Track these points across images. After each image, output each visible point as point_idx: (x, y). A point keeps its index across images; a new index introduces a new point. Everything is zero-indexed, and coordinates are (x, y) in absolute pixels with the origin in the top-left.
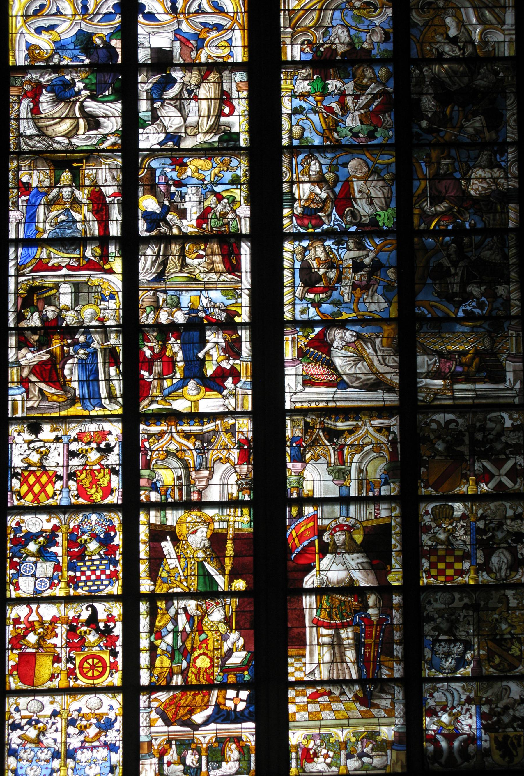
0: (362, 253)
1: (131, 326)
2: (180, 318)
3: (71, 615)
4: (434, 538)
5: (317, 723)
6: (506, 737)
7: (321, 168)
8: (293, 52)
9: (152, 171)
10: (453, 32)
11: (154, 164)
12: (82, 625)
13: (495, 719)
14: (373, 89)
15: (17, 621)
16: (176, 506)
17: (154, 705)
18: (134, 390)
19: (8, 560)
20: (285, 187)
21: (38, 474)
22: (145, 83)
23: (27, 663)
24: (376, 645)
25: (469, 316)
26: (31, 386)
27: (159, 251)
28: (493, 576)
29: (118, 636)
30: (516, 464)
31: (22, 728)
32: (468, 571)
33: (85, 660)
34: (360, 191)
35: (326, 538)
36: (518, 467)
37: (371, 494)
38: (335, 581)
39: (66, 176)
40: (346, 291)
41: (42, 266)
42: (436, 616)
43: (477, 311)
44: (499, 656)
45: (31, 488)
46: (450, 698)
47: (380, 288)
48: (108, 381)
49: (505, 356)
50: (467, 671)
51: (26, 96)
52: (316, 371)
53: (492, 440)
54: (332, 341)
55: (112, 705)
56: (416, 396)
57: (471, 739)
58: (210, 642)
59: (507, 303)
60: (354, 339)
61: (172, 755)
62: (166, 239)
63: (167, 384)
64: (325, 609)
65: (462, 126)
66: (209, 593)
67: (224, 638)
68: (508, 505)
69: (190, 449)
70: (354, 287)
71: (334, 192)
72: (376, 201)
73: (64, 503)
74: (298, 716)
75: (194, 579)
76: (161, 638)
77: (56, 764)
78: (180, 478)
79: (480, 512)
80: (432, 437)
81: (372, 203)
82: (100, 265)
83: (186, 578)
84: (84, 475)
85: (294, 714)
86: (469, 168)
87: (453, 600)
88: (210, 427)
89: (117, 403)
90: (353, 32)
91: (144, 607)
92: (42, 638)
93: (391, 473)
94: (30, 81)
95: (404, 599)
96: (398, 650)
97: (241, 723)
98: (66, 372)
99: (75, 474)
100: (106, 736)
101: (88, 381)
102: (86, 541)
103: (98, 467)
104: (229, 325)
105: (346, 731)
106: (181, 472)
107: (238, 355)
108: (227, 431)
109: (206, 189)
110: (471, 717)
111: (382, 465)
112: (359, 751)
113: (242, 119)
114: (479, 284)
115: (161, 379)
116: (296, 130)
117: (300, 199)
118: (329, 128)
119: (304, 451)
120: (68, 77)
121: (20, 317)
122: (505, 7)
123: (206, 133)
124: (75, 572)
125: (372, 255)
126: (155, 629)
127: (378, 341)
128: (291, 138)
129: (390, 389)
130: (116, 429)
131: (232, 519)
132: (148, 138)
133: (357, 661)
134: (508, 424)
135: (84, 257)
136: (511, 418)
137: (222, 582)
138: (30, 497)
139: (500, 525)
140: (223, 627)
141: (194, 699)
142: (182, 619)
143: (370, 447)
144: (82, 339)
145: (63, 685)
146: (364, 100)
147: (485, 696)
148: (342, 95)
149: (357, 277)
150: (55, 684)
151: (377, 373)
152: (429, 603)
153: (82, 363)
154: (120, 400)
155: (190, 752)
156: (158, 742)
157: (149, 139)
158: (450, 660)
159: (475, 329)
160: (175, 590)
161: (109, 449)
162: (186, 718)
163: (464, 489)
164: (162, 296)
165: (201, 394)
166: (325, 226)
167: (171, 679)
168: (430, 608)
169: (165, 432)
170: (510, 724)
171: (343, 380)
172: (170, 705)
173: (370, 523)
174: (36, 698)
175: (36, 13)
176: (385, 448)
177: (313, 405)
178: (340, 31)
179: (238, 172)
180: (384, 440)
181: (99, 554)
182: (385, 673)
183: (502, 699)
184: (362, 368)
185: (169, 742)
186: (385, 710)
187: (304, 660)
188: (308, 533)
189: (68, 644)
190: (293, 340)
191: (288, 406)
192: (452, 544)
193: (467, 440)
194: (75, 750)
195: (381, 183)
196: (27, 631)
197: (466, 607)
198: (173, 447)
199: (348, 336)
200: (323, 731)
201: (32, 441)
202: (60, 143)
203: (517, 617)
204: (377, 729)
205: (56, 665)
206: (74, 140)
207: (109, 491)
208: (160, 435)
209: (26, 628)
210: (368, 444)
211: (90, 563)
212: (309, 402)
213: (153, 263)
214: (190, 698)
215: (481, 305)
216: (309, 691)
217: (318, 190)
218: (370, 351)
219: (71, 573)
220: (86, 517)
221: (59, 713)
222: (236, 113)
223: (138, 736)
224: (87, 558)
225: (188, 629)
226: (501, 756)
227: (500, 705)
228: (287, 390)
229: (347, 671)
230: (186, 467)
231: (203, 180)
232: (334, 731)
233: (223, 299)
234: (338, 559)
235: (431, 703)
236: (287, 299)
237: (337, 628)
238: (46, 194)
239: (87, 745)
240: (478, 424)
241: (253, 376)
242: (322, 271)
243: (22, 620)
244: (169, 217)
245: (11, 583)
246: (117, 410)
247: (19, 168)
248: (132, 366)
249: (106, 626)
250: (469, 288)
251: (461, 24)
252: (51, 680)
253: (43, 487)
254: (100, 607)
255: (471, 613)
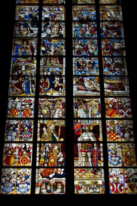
0: (91, 60)
1: (38, 76)
2: (49, 74)
3: (20, 146)
4: (110, 129)
5: (82, 179)
6: (131, 185)
7: (81, 42)
8: (75, 19)
9: (44, 42)
10: (109, 16)
11: (45, 40)
12: (23, 149)
13: (128, 179)
14: (92, 26)
15: (6, 147)
16: (47, 119)
17: (40, 172)
18: (38, 90)
19: (6, 131)
20: (73, 46)
21: (14, 110)
22: (43, 24)
23: (8, 159)
24: (96, 157)
25: (116, 75)
26: (14, 89)
27: (45, 59)
28: (125, 139)
29: (31, 152)
30: (129, 111)
31: (5, 177)
32: (119, 138)
33: (22, 159)
34: (90, 47)
35: (83, 128)
36: (130, 112)
37: (94, 117)
38: (86, 139)
39: (25, 42)
40: (87, 69)
41: (19, 61)
42: (111, 150)
43: (118, 74)
44: (128, 161)
45: (12, 113)
46: (116, 173)
47: (95, 68)
48: (32, 88)
49: (125, 85)
50: (120, 165)
51: (18, 26)
52: (80, 87)
53: (123, 105)
54: (84, 80)
55: (29, 172)
56: (104, 93)
57: (122, 185)
58: (54, 155)
59: (124, 72)
60: (89, 80)
61: (44, 186)
62: (47, 56)
63: (46, 89)
64: (83, 147)
65: (112, 34)
66: (54, 142)
67: (58, 154)
68: (128, 121)
69: (50, 105)
70: (89, 68)
71: (84, 47)
72: (93, 49)
73: (20, 117)
74: (77, 177)
75: (51, 138)
76: (42, 153)
77: (14, 188)
78: (48, 112)
79: (121, 123)
80: (108, 103)
81: (93, 50)
82: (32, 61)
83: (49, 137)
84: (25, 110)
85: (76, 176)
86: (114, 43)
87: (116, 145)
88: (55, 99)
89: (34, 93)
90: (87, 15)
91: (38, 145)
92: (12, 152)
93: (99, 112)
94: (19, 23)
95: (103, 145)
96: (102, 159)
97: (62, 178)
98: (22, 85)
99: (23, 110)
100: (27, 180)
101: (27, 88)
102: (25, 127)
103: (28, 108)
104: (60, 76)
105: (90, 181)
106: (48, 110)
107: (62, 83)
108: (59, 101)
109: (56, 46)
110: (122, 178)
111: (97, 110)
112: (93, 187)
113: (64, 32)
114: (118, 68)
115: (44, 88)
116: (75, 34)
117: (77, 48)
118: (83, 34)
119: (78, 106)
120: (27, 23)
121: (13, 73)
122: (120, 11)
123: (56, 34)
124: (22, 135)
125: (93, 61)
126: (41, 151)
127: (95, 80)
128: (74, 36)
129: (98, 92)
130: (33, 99)
131: (60, 122)
132: (43, 35)
133: (92, 161)
134: (127, 101)
135: (28, 60)
136: (127, 99)
137: (57, 138)
138: (12, 115)
139: (126, 126)
140: (58, 151)
141: (50, 170)
142: (47, 148)
143: (94, 105)
144: (26, 78)
145: (17, 165)
146: (90, 29)
147: (125, 172)
148: (86, 27)
149: (90, 66)
150: (15, 165)
151: (95, 88)
152: (110, 146)
153: (26, 84)
154: (35, 92)
155: (48, 186)
156: (40, 182)
157: (44, 35)
158: (115, 162)
159: (117, 78)
160: (46, 141)
161: (31, 104)
162: (47, 176)
163: (117, 117)
164: (45, 69)
165: (53, 92)
166: (82, 54)
167: (44, 165)
168: (110, 148)
169: (45, 100)
170: (132, 181)
171: (87, 89)
172: (44, 172)
173: (94, 125)
174: (10, 169)
175: (21, 10)
176: (97, 106)
177: (80, 95)
178: (85, 15)
179: (63, 43)
180: (97, 104)
181: (28, 130)
182: (99, 165)
183: (129, 173)
184: (91, 86)
185: (43, 183)
186: (99, 176)
187: (78, 161)
188: (79, 127)
189: (19, 154)
190: (75, 79)
191: (74, 95)
192: (115, 131)
193: (117, 104)
194: (19, 184)
195: (94, 46)
196: (9, 150)
197: (119, 147)
198: (46, 104)
199: (88, 79)
200: (83, 181)
201: (14, 102)
202: (24, 36)
203: (132, 151)
204: (97, 181)
205: (15, 160)
206: (27, 35)
207: (31, 114)
208: (43, 101)
209: (9, 149)
210: (93, 105)
211: (25, 133)
212: (79, 94)
213: (43, 62)
214: (49, 170)
215: (118, 73)
216: (79, 170)
217: (81, 47)
218: (93, 82)
219: (21, 135)
220: (25, 121)
221: (15, 173)
222: (63, 30)
223: (35, 181)
224: (25, 131)
225: (49, 151)
226: (130, 190)
227: (129, 175)
228: (74, 91)
229: (89, 164)
230: (49, 109)
231: (55, 44)
232: (86, 181)
233: (59, 70)
234: (87, 134)
235: (111, 174)
236: (74, 70)
237: (86, 152)
238: (21, 46)
239: (22, 182)
240: (119, 101)
241: (66, 88)
242: (82, 64)
243: (8, 147)
244: (47, 52)
245: (6, 137)
246: (34, 95)
247: (15, 41)
248: (38, 84)
249: (28, 150)
250: (116, 69)
251: (111, 14)
252: (14, 164)
253: (15, 113)
254: (27, 144)
255: (120, 149)
